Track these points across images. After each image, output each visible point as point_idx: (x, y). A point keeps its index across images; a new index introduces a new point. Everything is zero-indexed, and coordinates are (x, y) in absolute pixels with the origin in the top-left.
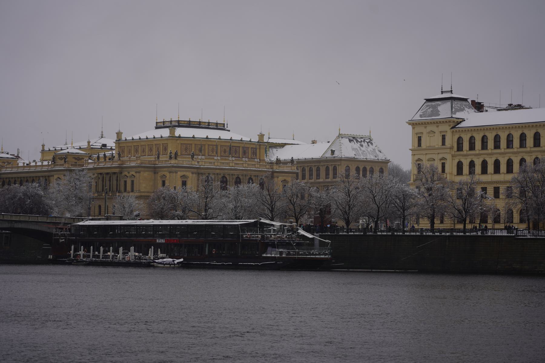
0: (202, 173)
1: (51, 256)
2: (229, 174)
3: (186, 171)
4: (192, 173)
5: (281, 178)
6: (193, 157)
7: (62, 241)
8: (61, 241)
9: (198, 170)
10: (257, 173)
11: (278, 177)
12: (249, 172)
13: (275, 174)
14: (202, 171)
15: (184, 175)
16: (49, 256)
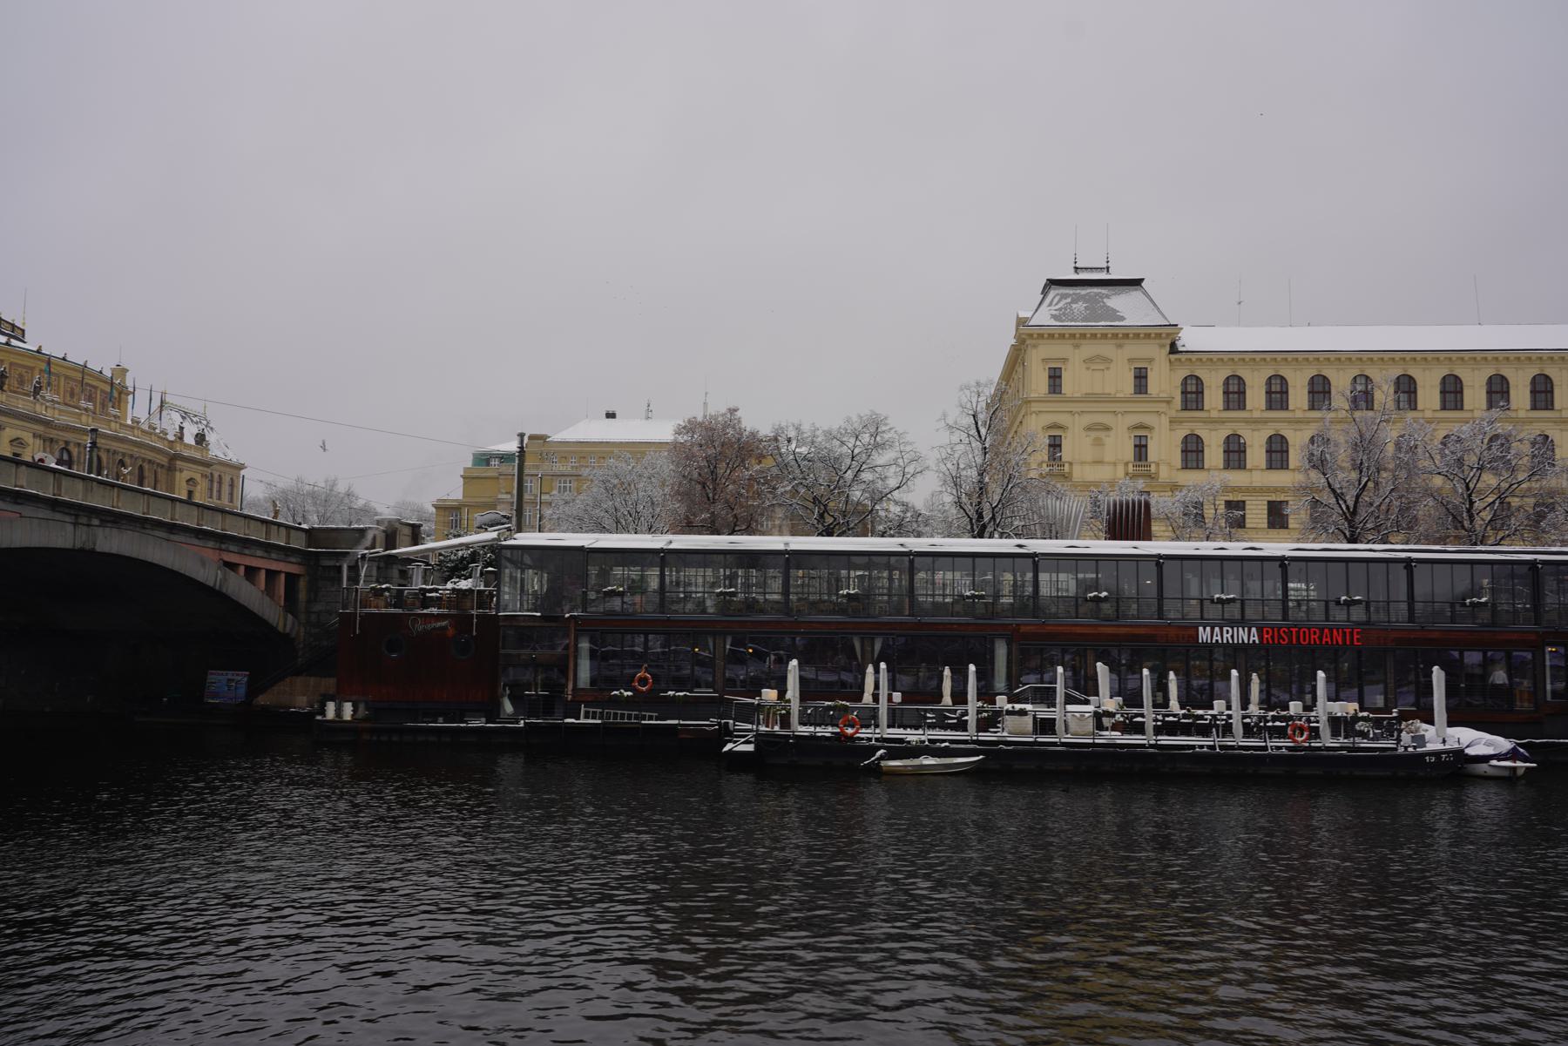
0: (52, 440)
1: (348, 709)
2: (108, 451)
3: (23, 429)
4: (35, 436)
5: (186, 475)
6: (37, 390)
7: (429, 627)
8: (420, 628)
9: (48, 430)
10: (152, 454)
11: (181, 471)
12: (143, 451)
13: (178, 463)
14: (54, 434)
15: (18, 439)
16: (331, 708)
